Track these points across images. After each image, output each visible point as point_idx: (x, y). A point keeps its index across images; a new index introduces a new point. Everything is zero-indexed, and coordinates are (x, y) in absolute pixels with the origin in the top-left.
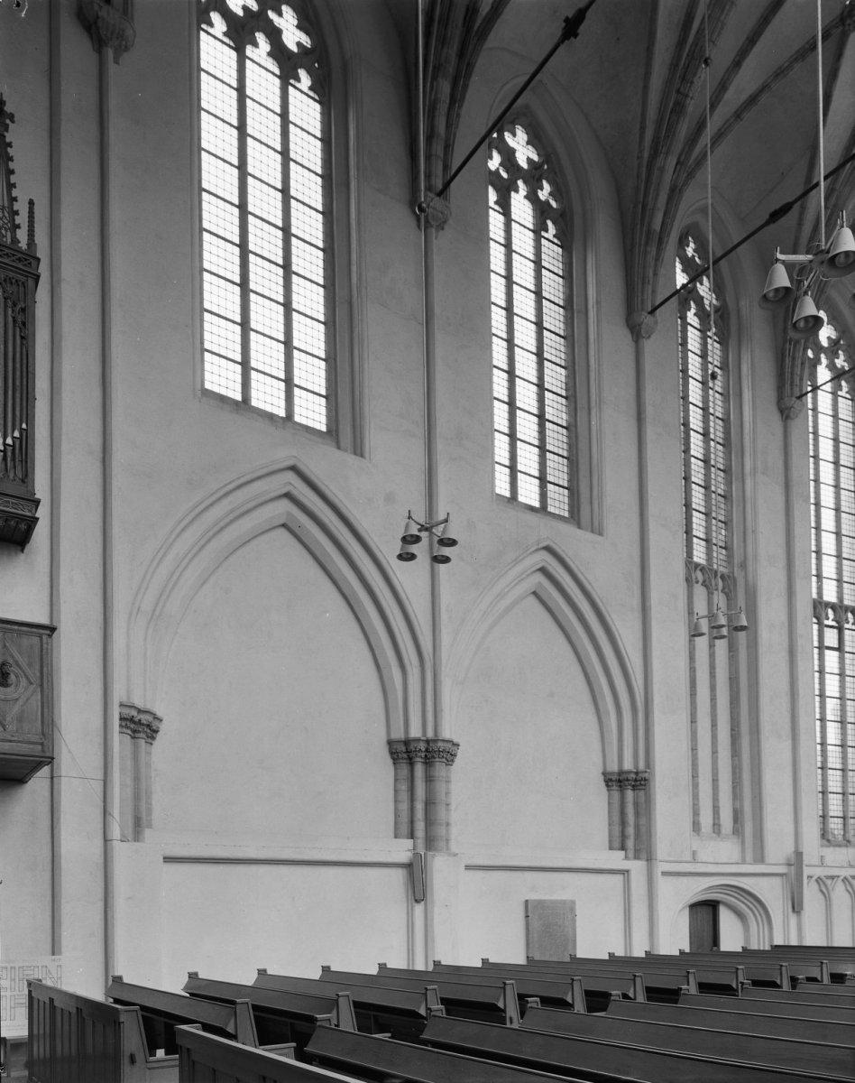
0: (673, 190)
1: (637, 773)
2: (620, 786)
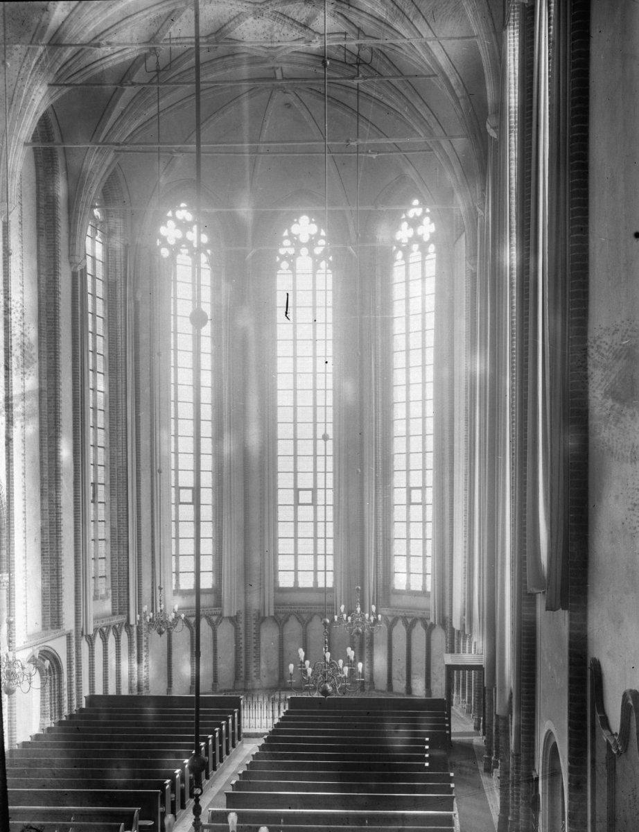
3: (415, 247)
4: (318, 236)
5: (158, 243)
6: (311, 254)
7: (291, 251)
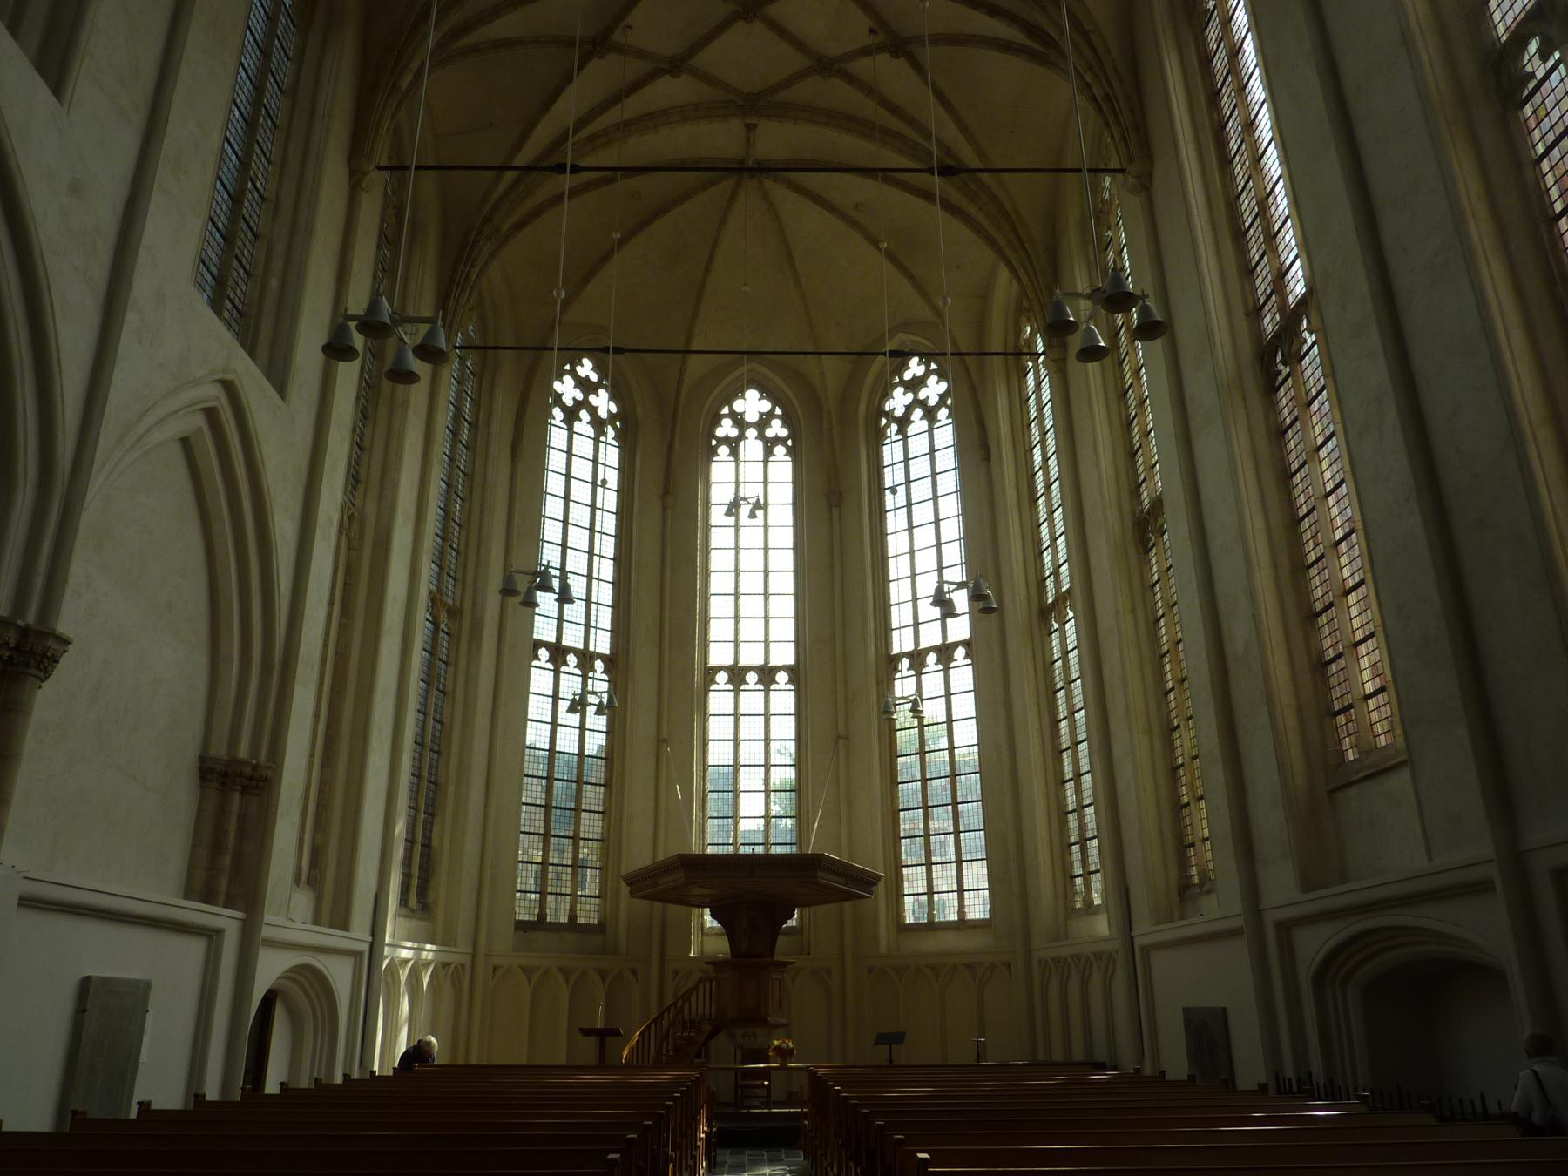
1: (255, 767)
2: (223, 784)
3: (917, 413)
6: (761, 436)
7: (734, 433)
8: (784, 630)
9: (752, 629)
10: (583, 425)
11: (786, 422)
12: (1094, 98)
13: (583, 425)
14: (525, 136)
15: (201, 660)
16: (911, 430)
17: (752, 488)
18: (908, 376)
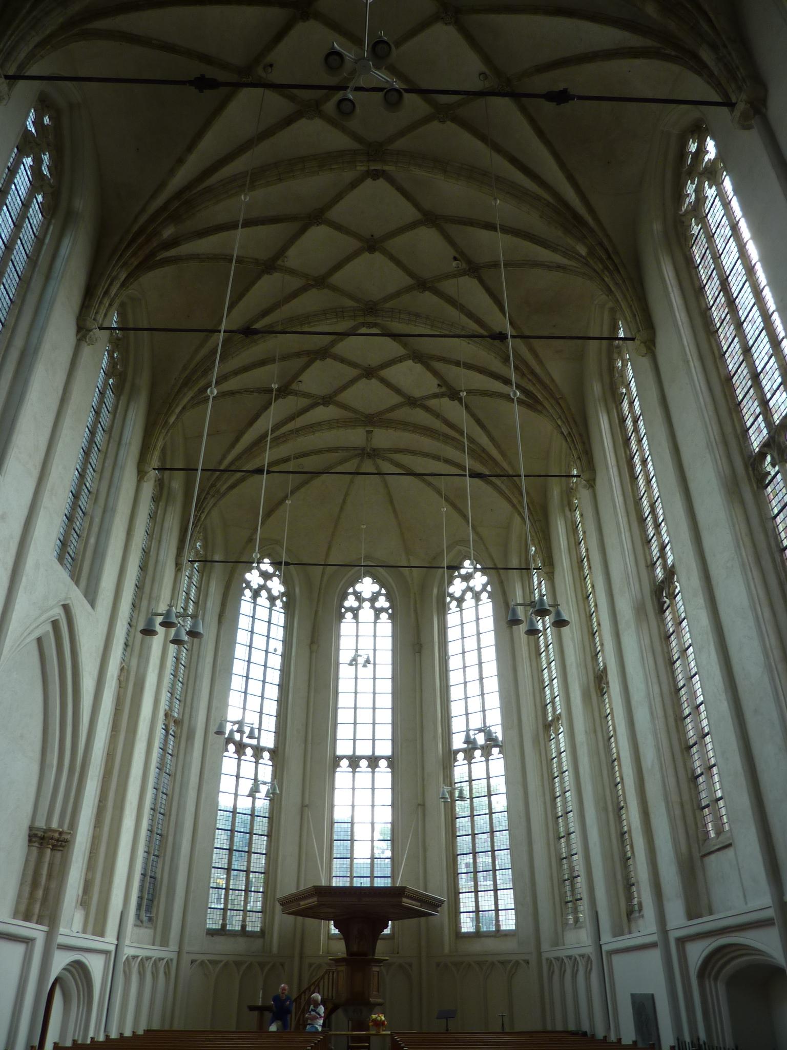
0: (184, 408)
1: (61, 833)
2: (41, 844)
3: (469, 595)
4: (378, 594)
5: (244, 585)
6: (373, 607)
7: (356, 604)
8: (385, 732)
9: (364, 732)
10: (263, 600)
11: (389, 597)
12: (562, 433)
13: (263, 600)
14: (237, 439)
15: (36, 767)
16: (464, 605)
17: (366, 635)
18: (463, 572)
